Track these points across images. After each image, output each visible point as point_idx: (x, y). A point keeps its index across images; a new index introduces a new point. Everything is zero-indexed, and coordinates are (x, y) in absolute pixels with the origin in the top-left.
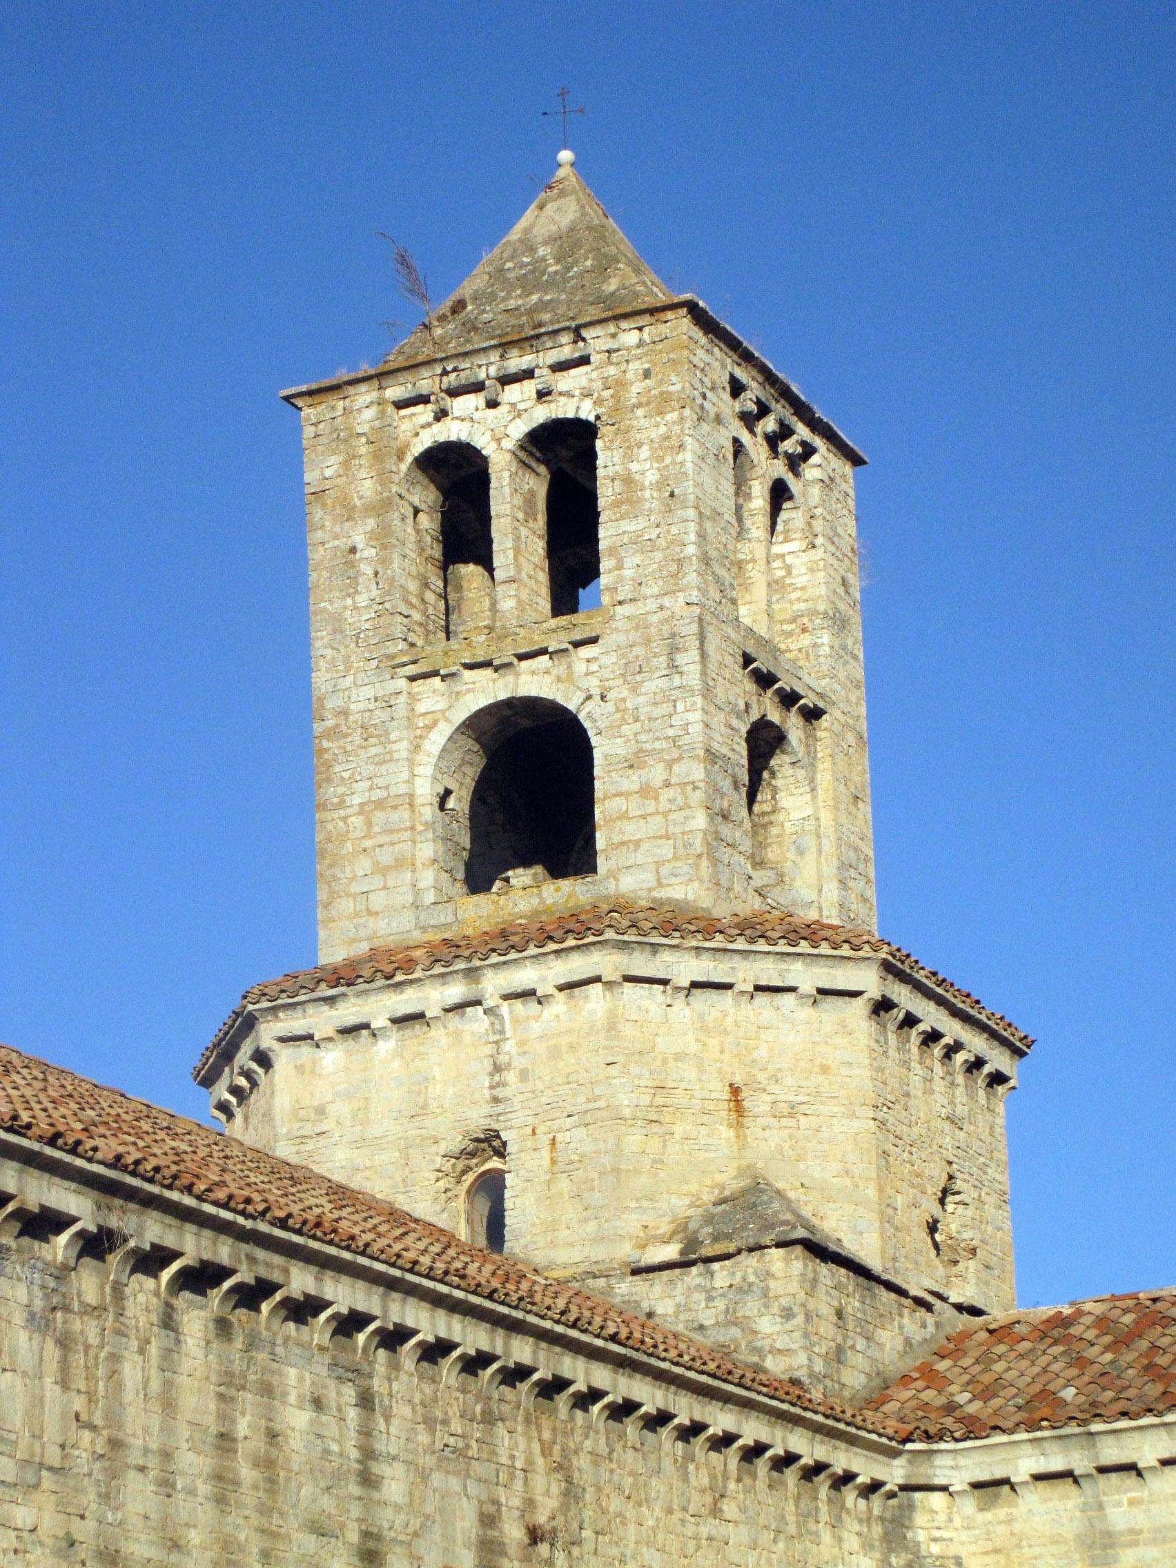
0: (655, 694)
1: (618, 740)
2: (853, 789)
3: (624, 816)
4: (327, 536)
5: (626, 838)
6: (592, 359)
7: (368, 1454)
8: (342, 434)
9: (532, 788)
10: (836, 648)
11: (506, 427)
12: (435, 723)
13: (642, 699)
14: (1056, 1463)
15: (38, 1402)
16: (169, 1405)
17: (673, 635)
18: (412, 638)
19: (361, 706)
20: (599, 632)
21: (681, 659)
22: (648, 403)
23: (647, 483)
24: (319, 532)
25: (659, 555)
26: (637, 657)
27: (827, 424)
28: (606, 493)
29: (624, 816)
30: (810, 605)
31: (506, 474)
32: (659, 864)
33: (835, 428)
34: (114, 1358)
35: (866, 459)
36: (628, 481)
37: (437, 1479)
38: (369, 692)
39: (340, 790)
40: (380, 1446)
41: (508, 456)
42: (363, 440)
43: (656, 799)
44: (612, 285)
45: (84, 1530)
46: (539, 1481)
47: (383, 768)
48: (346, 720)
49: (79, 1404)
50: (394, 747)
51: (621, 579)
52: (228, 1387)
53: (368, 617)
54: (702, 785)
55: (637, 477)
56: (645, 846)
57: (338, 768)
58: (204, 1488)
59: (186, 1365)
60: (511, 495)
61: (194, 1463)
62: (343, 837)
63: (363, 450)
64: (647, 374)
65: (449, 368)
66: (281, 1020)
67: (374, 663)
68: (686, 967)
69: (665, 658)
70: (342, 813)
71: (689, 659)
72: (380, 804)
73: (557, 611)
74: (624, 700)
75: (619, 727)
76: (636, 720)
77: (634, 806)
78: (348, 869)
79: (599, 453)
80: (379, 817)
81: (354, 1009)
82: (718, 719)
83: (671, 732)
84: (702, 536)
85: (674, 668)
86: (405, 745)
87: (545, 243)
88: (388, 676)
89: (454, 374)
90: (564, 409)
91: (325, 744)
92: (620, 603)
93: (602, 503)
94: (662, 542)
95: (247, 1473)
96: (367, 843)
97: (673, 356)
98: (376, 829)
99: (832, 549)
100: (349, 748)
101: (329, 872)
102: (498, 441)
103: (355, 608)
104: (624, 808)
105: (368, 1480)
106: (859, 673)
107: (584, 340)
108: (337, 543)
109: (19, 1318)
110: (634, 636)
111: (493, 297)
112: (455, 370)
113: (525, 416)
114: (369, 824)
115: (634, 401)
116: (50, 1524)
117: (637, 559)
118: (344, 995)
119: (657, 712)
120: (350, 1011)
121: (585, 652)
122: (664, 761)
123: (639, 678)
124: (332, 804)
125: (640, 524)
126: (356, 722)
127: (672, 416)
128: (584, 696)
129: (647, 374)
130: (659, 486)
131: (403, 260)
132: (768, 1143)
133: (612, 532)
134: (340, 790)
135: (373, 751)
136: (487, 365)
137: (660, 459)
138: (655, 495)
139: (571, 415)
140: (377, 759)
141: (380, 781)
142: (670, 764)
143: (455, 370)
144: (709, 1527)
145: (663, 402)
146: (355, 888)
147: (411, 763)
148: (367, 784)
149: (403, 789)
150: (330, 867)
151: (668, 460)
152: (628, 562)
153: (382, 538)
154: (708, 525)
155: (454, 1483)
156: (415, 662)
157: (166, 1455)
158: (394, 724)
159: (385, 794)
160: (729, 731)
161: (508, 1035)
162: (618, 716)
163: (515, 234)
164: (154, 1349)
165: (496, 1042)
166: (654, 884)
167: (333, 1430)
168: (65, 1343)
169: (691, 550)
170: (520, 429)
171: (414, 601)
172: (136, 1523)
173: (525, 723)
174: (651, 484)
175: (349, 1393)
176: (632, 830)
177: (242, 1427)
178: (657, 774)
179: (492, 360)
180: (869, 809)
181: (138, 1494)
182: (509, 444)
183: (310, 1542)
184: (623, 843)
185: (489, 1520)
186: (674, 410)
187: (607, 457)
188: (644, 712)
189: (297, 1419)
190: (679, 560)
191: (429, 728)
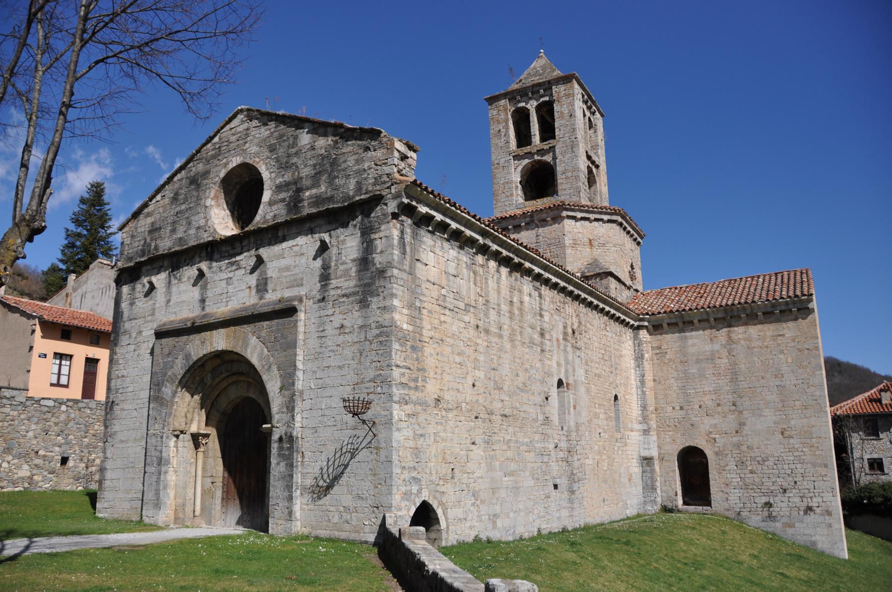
7: (541, 309)
9: (540, 180)
14: (673, 321)
15: (469, 288)
16: (499, 292)
28: (556, 114)
34: (486, 279)
36: (562, 112)
37: (555, 316)
40: (543, 307)
45: (481, 323)
46: (574, 319)
49: (479, 290)
52: (512, 289)
58: (507, 315)
59: (502, 283)
61: (505, 308)
68: (579, 215)
90: (547, 99)
95: (516, 312)
105: (541, 316)
109: (464, 266)
116: (473, 322)
131: (511, 69)
132: (597, 252)
144: (605, 332)
155: (558, 318)
157: (499, 305)
163: (532, 66)
164: (495, 278)
167: (533, 303)
168: (475, 273)
172: (492, 323)
175: (537, 293)
177: (515, 300)
178: (569, 174)
181: (493, 314)
183: (530, 330)
185: (565, 327)
187: (556, 107)
189: (526, 299)
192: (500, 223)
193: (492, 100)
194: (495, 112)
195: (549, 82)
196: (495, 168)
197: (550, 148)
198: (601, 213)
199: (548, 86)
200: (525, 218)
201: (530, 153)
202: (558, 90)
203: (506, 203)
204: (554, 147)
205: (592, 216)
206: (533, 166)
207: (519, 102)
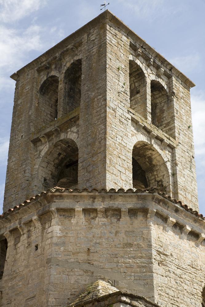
55: (182, 115)
63: (122, 45)
65: (144, 47)
66: (160, 206)
81: (182, 218)
92: (180, 143)
101: (110, 156)
103: (118, 84)
110: (182, 155)
118: (182, 212)
120: (181, 219)
123: (185, 167)
124: (111, 135)
140: (124, 133)
142: (192, 196)
143: (145, 49)
148: (121, 138)
156: (133, 114)
159: (126, 146)
170: (153, 77)
192: (177, 210)
194: (114, 41)
195: (172, 68)
207: (137, 56)
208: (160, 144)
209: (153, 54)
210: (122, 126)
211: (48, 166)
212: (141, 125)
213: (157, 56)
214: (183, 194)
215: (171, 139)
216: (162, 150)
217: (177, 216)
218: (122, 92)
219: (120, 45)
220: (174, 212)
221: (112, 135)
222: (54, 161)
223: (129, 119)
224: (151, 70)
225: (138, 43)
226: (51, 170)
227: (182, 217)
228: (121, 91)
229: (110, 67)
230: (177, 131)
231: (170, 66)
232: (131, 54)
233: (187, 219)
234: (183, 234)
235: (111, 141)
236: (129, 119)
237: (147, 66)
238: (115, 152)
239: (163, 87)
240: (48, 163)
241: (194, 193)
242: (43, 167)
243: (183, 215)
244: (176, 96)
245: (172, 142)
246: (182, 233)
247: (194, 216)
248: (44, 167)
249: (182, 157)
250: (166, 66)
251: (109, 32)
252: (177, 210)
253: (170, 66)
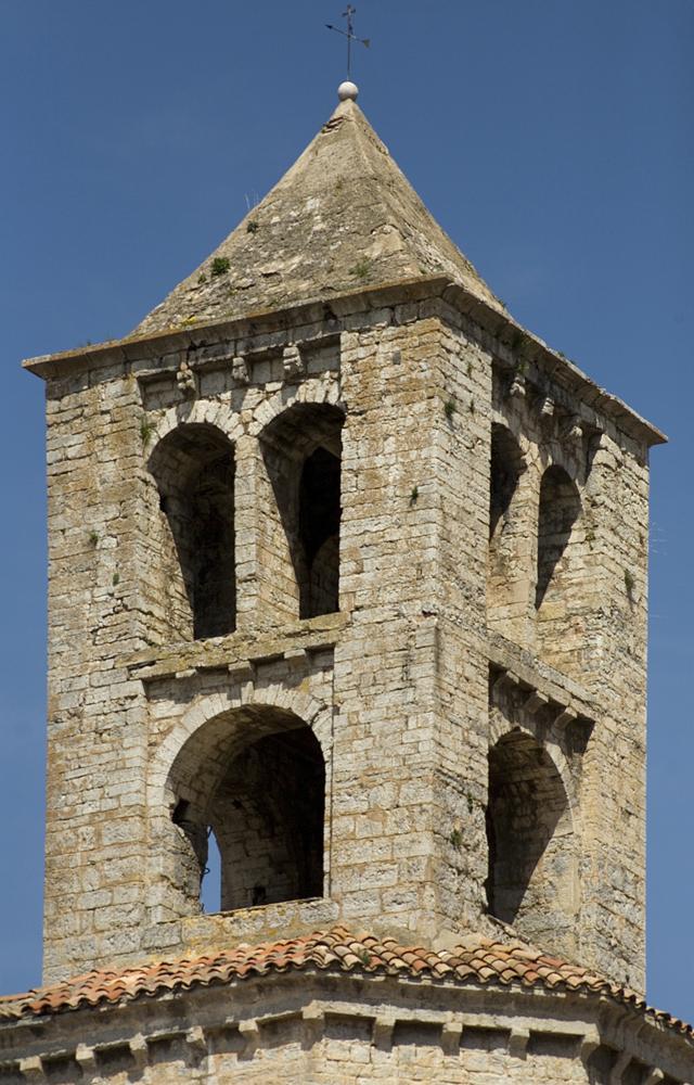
0: (388, 708)
1: (349, 756)
2: (623, 804)
3: (352, 837)
4: (69, 525)
5: (351, 861)
6: (343, 339)
8: (86, 410)
10: (612, 649)
11: (253, 409)
12: (170, 729)
13: (374, 714)
17: (408, 647)
18: (152, 636)
19: (97, 708)
20: (335, 639)
21: (416, 672)
22: (397, 391)
23: (391, 479)
24: (60, 517)
25: (399, 558)
26: (372, 668)
27: (615, 401)
29: (352, 837)
30: (584, 603)
31: (252, 462)
32: (383, 890)
33: (626, 406)
35: (666, 437)
36: (373, 475)
38: (103, 694)
39: (72, 798)
41: (255, 442)
42: (108, 418)
43: (384, 822)
44: (375, 251)
47: (113, 778)
48: (81, 723)
50: (127, 754)
51: (359, 583)
53: (103, 613)
54: (429, 807)
55: (381, 472)
56: (372, 870)
57: (70, 775)
60: (257, 485)
62: (72, 850)
63: (107, 429)
64: (396, 360)
65: (197, 343)
67: (110, 663)
69: (400, 669)
70: (72, 823)
71: (423, 672)
72: (110, 814)
73: (307, 612)
74: (357, 713)
75: (351, 742)
76: (368, 734)
77: (359, 827)
78: (75, 886)
79: (345, 444)
80: (109, 832)
81: (60, 1039)
82: (453, 739)
83: (402, 750)
84: (445, 538)
85: (409, 682)
86: (139, 751)
87: (315, 195)
88: (124, 678)
89: (203, 349)
90: (313, 391)
91: (59, 748)
92: (357, 609)
93: (344, 499)
94: (403, 545)
96: (97, 857)
97: (424, 339)
98: (106, 841)
99: (616, 540)
100: (82, 754)
102: (246, 425)
104: (352, 828)
106: (640, 675)
107: (335, 317)
108: (77, 530)
110: (370, 646)
111: (255, 259)
112: (203, 344)
113: (274, 398)
114: (99, 835)
115: (382, 388)
117: (377, 563)
119: (389, 727)
121: (321, 661)
122: (394, 780)
123: (373, 690)
124: (62, 813)
125: (384, 521)
126: (90, 726)
127: (420, 407)
128: (319, 706)
129: (396, 360)
130: (404, 482)
133: (354, 530)
134: (72, 798)
135: (106, 757)
136: (236, 341)
137: (406, 453)
138: (398, 493)
139: (319, 400)
140: (109, 767)
141: (112, 791)
143: (203, 344)
145: (407, 391)
146: (82, 904)
147: (146, 772)
148: (96, 793)
149: (135, 799)
150: (58, 880)
151: (413, 455)
152: (367, 565)
153: (124, 530)
154: (453, 526)
156: (152, 663)
158: (128, 728)
160: (467, 748)
161: (210, 1072)
162: (350, 729)
163: (286, 182)
165: (199, 1079)
166: (377, 911)
169: (432, 554)
171: (156, 595)
173: (266, 730)
174: (395, 481)
176: (359, 854)
178: (385, 795)
179: (241, 336)
180: (643, 824)
182: (255, 429)
184: (348, 867)
186: (422, 399)
187: (353, 452)
188: (375, 728)
190: (419, 564)
191: (164, 734)
193: (68, 374)
194: (75, 444)
195: (328, 312)
196: (68, 737)
197: (313, 652)
198: (493, 1005)
199: (317, 327)
200: (151, 1013)
201: (222, 670)
202: (369, 351)
203: (103, 920)
204: (328, 650)
205: (453, 1021)
206: (241, 728)
207: (190, 396)
208: (287, 671)
209: (236, 331)
210: (106, 747)
211: (248, 848)
212: (184, 679)
213: (253, 326)
214: (353, 805)
215: (317, 622)
216: (294, 685)
217: (45, 1042)
218: (105, 622)
219: (98, 437)
220: (33, 1037)
221: (66, 809)
222: (248, 827)
223: (133, 698)
224: (262, 387)
225: (173, 349)
226: (265, 852)
227: (61, 1034)
228: (104, 617)
229: (64, 563)
230: (352, 566)
231: (316, 308)
232: (170, 407)
233: (76, 1030)
234: (85, 1075)
235: (63, 829)
236: (133, 698)
237: (238, 393)
238: (78, 859)
239: (326, 404)
240: (243, 842)
241: (409, 767)
242: (235, 862)
243: (59, 1030)
244: (354, 414)
245: (321, 631)
246: (82, 1074)
247: (86, 1013)
248: (238, 861)
249: (366, 656)
250: (305, 319)
251: (58, 424)
252: (37, 1031)
253: (316, 308)
